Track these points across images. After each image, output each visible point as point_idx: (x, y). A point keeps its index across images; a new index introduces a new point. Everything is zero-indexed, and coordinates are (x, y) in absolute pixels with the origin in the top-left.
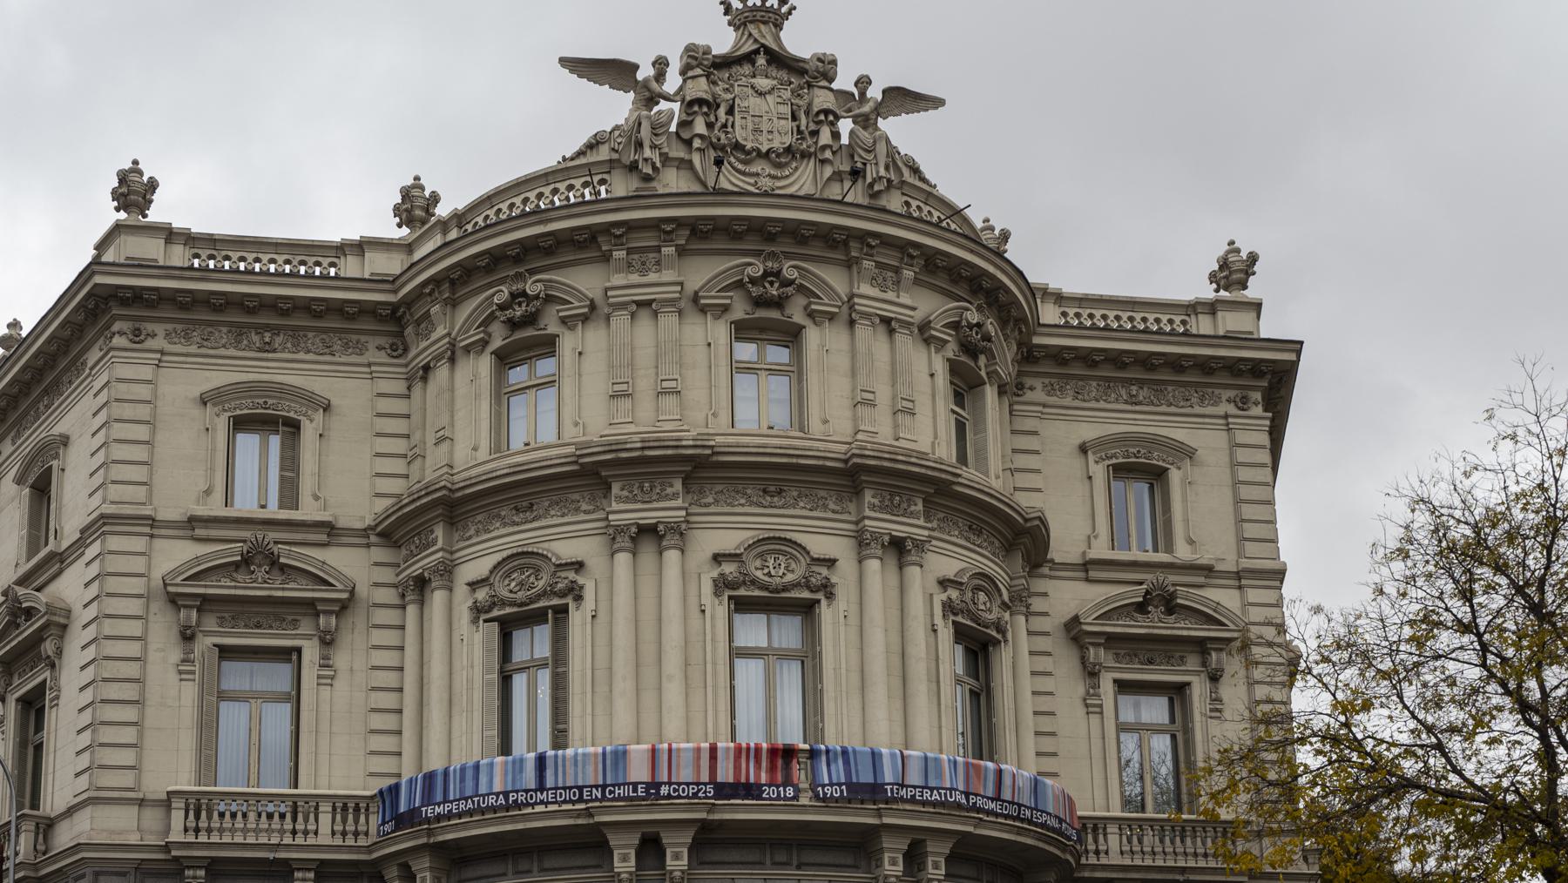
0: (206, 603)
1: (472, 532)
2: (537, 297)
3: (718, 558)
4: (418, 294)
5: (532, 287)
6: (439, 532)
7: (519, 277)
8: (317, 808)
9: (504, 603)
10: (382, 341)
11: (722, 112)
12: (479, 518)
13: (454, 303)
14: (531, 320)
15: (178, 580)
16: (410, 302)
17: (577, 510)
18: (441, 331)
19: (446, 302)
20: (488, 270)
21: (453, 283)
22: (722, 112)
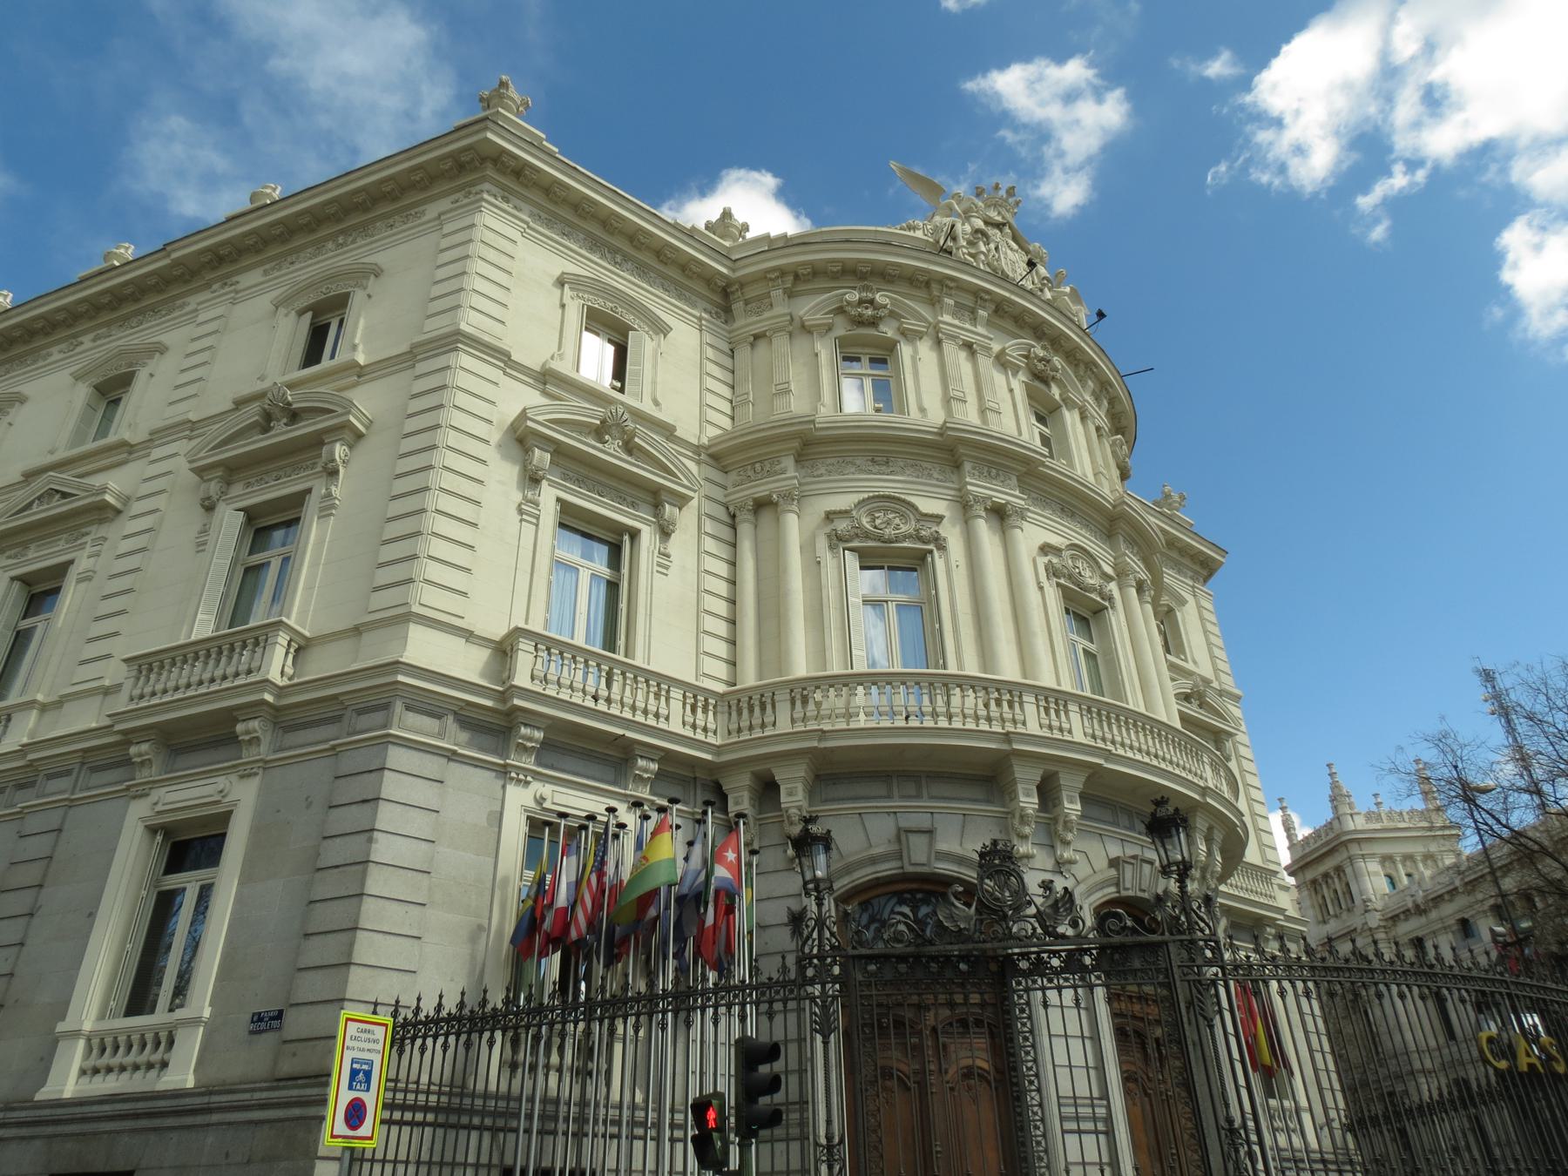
0: (561, 453)
1: (822, 471)
2: (885, 306)
3: (1045, 549)
4: (764, 277)
5: (880, 298)
6: (789, 463)
7: (867, 289)
8: (668, 692)
9: (867, 536)
10: (709, 307)
11: (992, 246)
12: (829, 461)
13: (791, 294)
14: (873, 323)
15: (540, 418)
16: (742, 285)
17: (930, 476)
18: (781, 309)
19: (785, 291)
20: (835, 276)
21: (797, 277)
22: (992, 246)
